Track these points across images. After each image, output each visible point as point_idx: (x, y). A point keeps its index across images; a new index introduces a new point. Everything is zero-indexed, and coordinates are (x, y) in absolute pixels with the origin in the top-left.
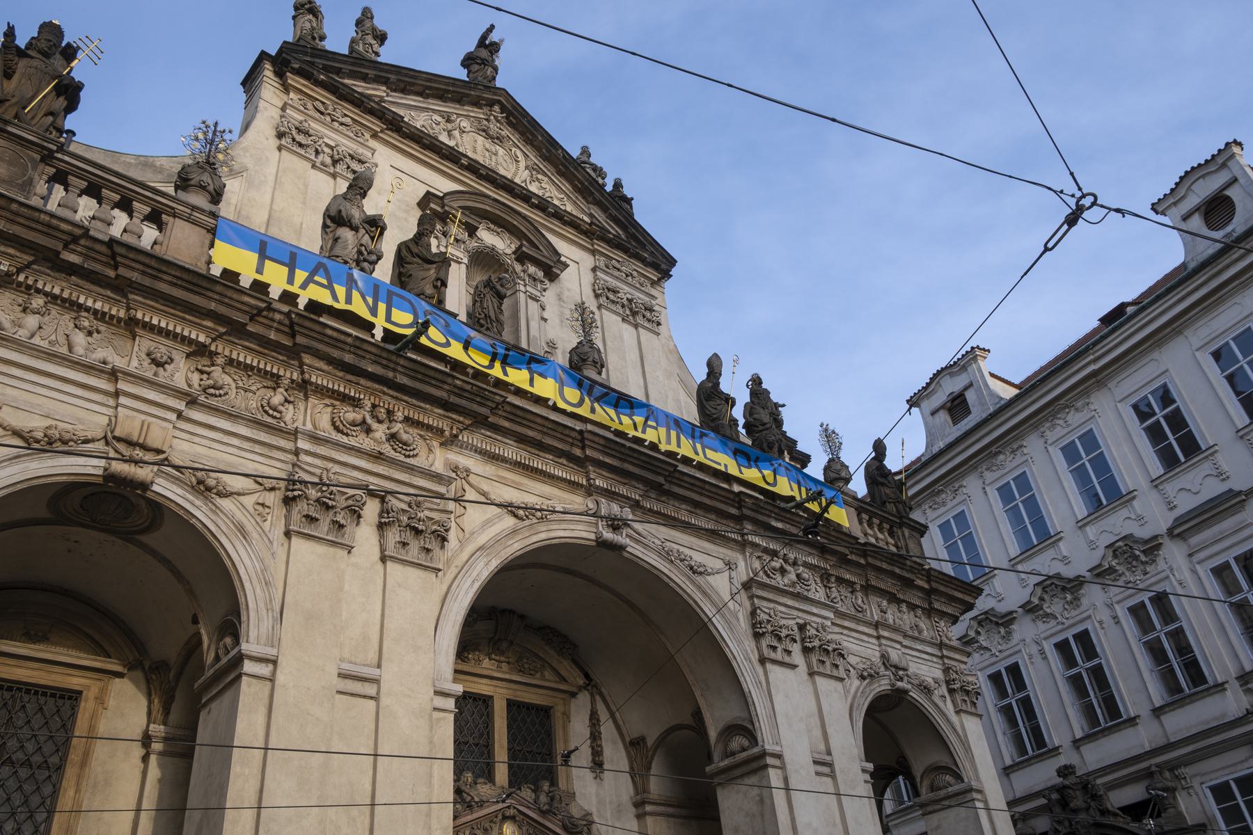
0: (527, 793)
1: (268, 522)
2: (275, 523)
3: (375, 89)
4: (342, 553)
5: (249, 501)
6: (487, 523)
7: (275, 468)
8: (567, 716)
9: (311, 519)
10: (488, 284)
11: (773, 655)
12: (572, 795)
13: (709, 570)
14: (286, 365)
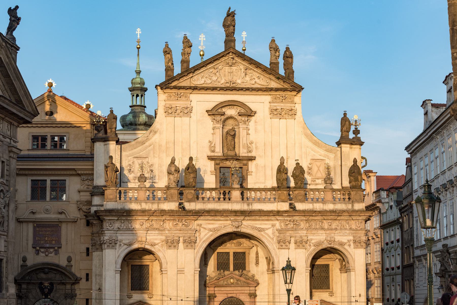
0: (237, 272)
1: (163, 248)
2: (165, 248)
3: (189, 76)
4: (176, 250)
5: (160, 244)
6: (206, 235)
7: (163, 238)
8: (249, 254)
9: (170, 246)
10: (227, 133)
11: (281, 247)
12: (250, 271)
13: (265, 229)
14: (162, 217)
